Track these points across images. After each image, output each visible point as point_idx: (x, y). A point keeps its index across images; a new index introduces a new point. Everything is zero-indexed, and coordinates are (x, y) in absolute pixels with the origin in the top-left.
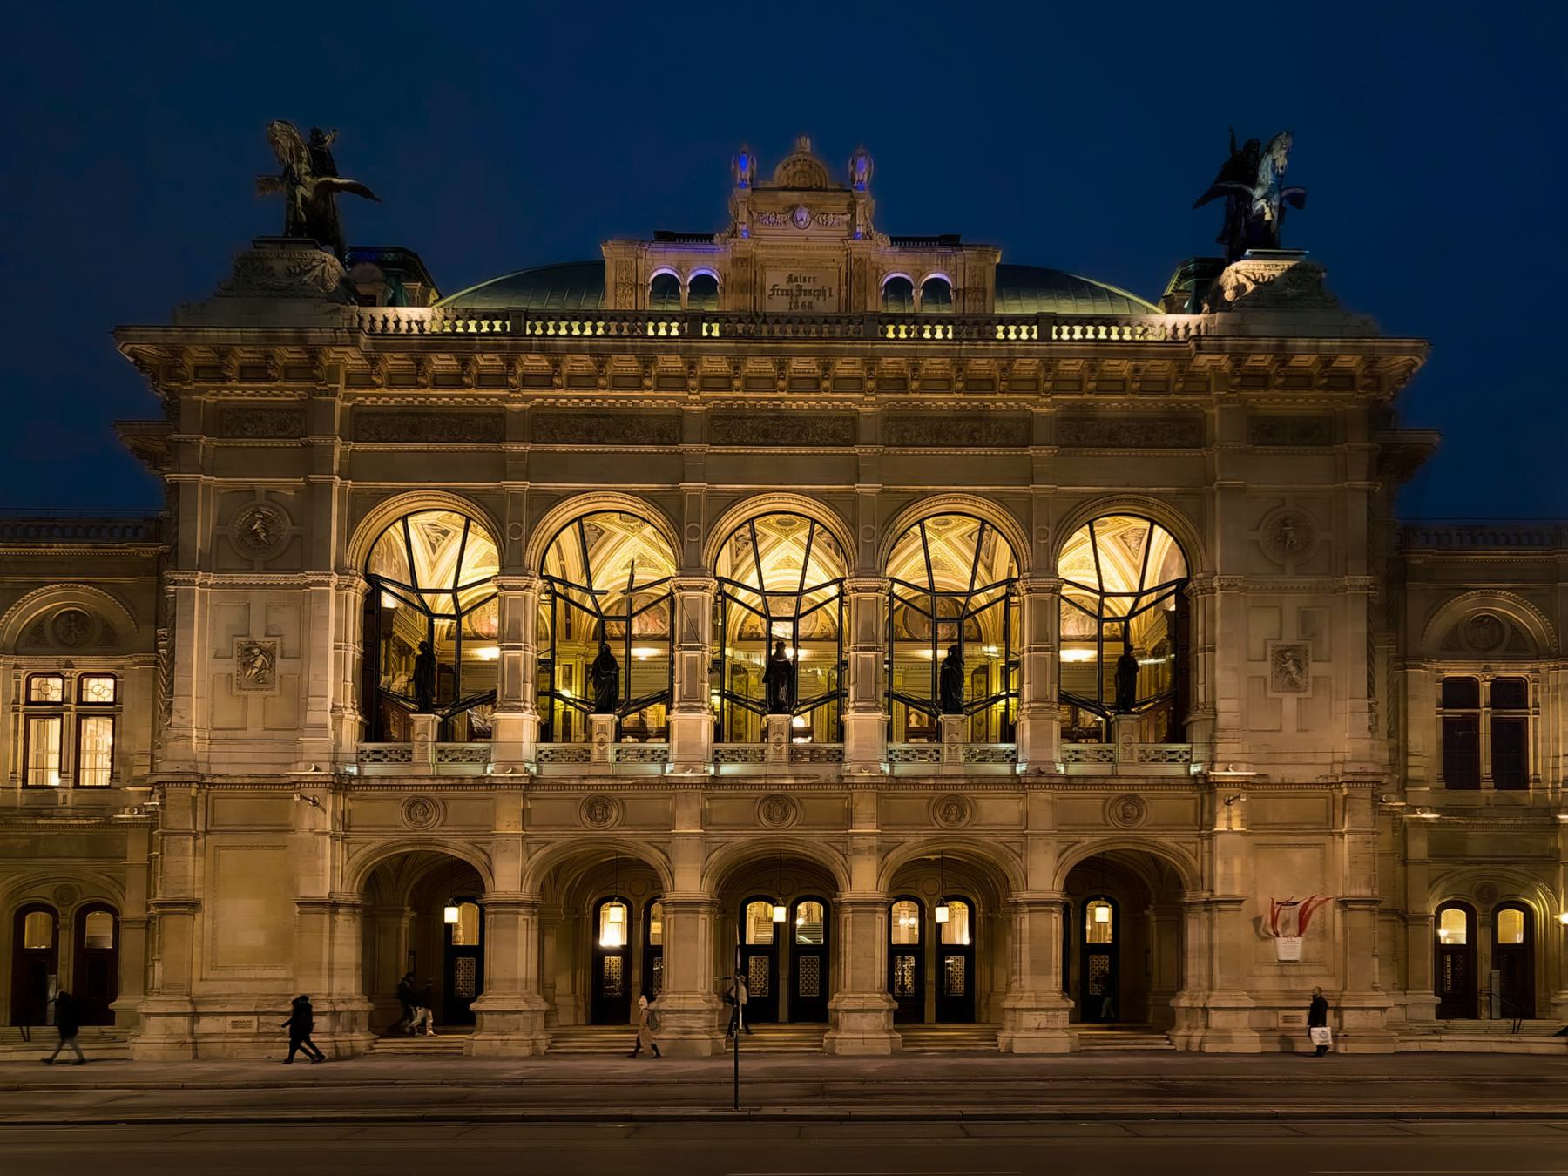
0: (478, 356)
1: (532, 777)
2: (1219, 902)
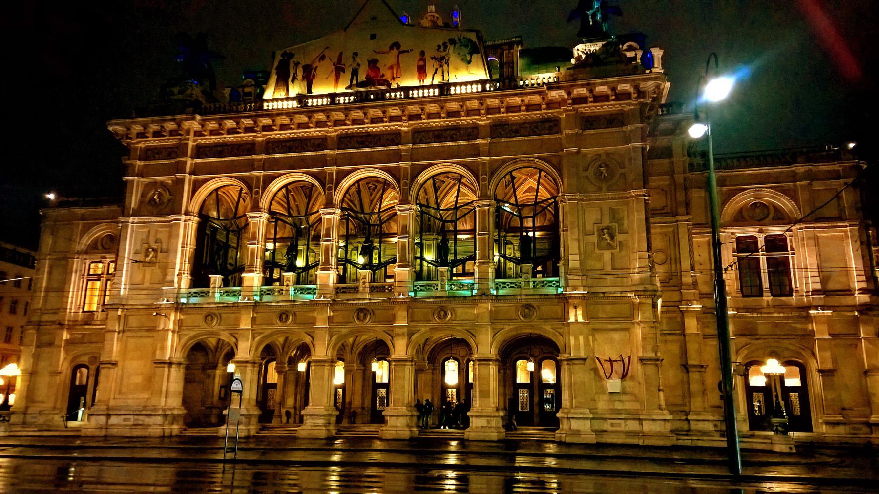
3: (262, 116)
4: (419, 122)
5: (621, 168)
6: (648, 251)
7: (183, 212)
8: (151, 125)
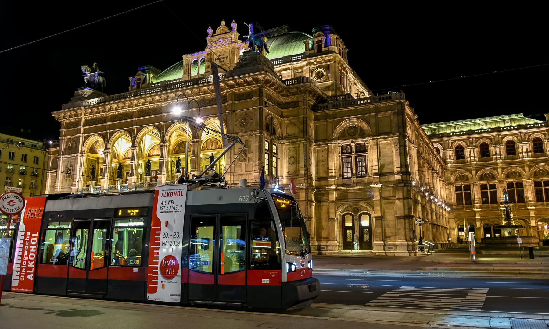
5: (251, 120)
7: (79, 152)
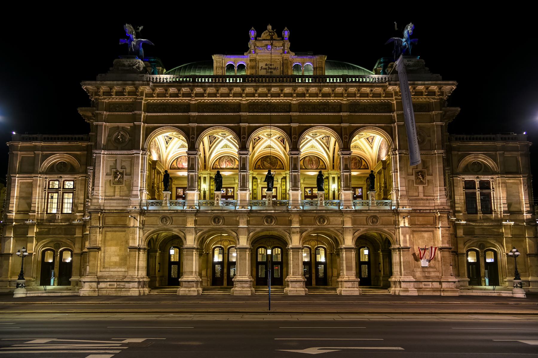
0: (183, 88)
1: (197, 210)
2: (402, 248)
3: (198, 86)
4: (303, 98)
6: (445, 186)
8: (115, 87)
